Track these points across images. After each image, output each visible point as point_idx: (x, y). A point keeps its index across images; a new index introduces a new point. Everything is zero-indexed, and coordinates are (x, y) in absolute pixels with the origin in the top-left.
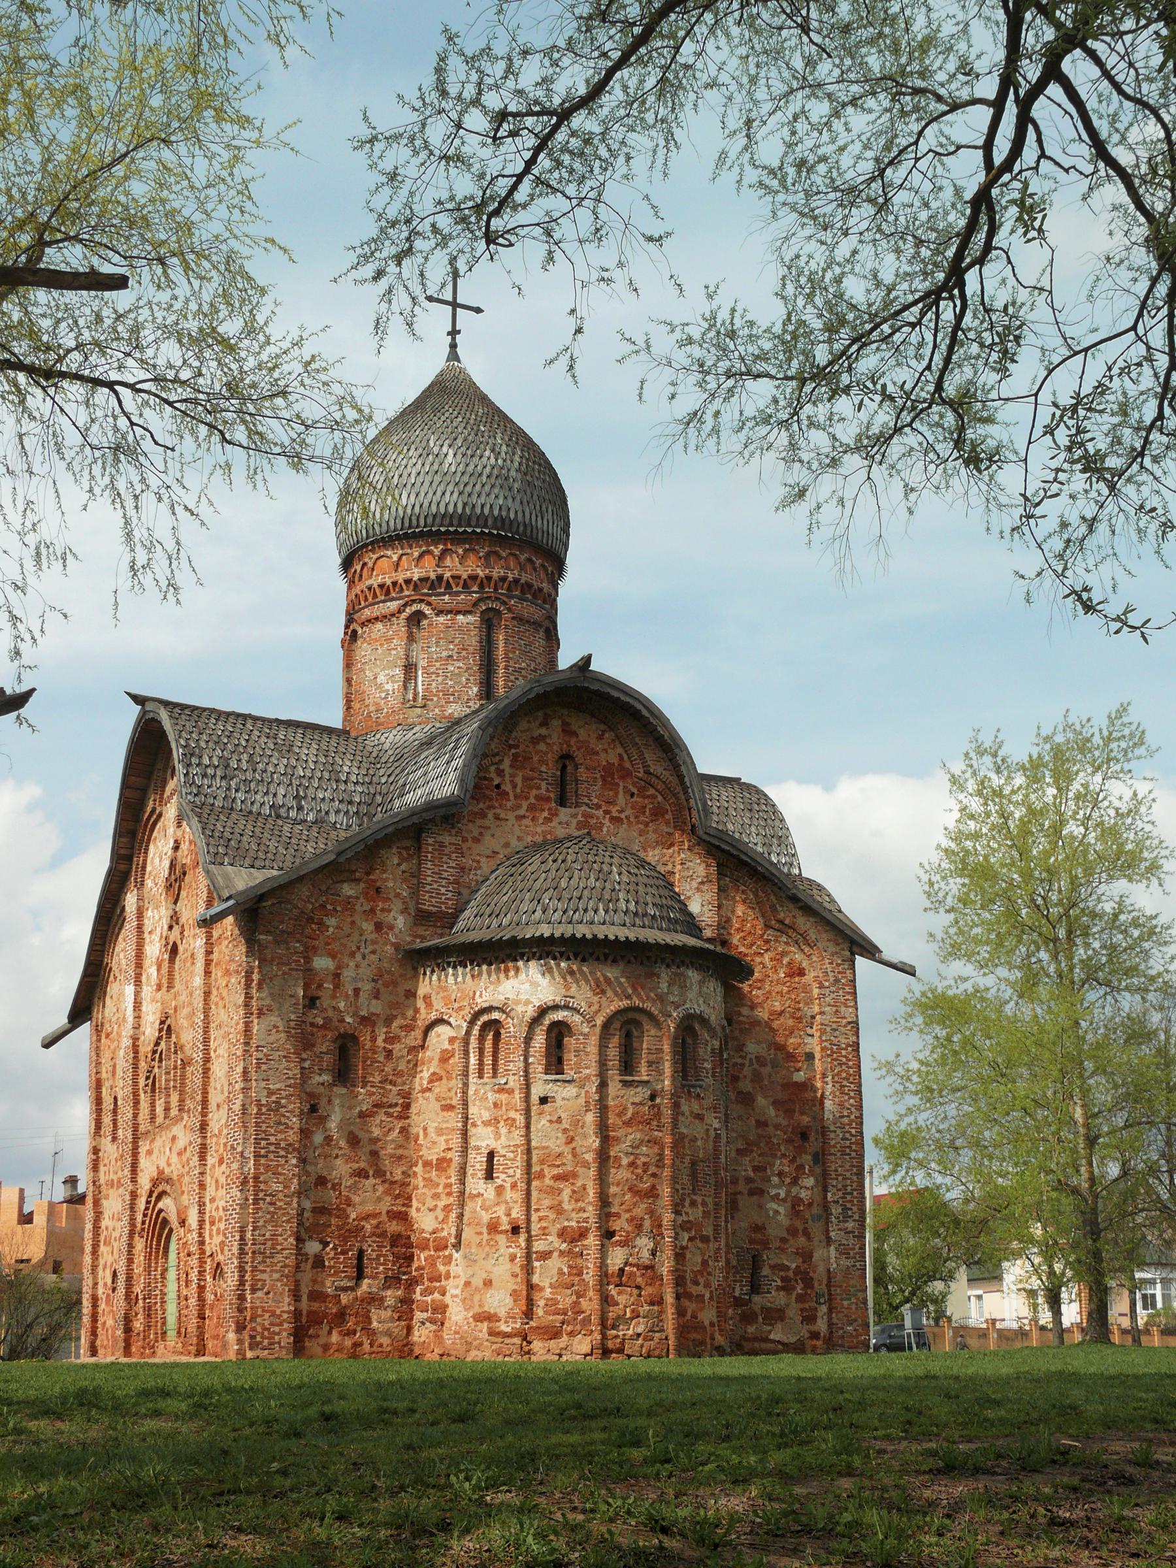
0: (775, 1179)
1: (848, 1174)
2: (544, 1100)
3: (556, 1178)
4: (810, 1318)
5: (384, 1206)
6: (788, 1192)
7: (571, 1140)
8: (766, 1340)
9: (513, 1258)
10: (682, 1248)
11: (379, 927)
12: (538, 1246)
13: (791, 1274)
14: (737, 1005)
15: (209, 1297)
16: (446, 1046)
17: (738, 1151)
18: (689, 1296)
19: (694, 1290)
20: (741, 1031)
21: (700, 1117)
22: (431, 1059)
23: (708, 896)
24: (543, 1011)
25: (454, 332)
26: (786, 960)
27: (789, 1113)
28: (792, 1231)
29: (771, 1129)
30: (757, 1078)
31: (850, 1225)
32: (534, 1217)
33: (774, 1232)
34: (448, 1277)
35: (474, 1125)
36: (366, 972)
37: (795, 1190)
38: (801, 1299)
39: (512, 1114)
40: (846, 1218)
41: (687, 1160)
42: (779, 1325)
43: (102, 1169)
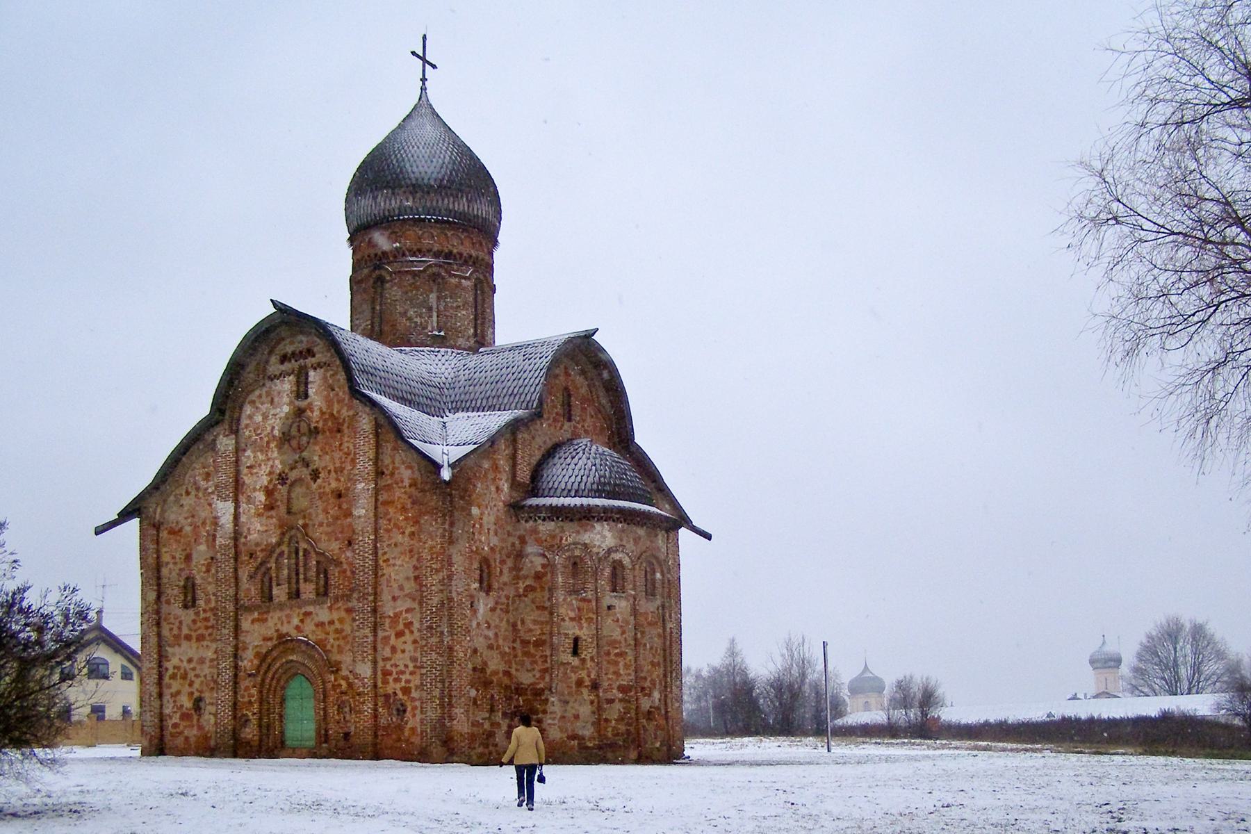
2: (609, 608)
3: (617, 655)
5: (502, 667)
7: (623, 633)
9: (592, 702)
11: (498, 489)
12: (609, 696)
15: (383, 722)
16: (539, 568)
22: (526, 577)
24: (610, 551)
25: (424, 80)
32: (605, 677)
34: (545, 712)
35: (563, 620)
36: (492, 519)
39: (591, 615)
43: (164, 624)
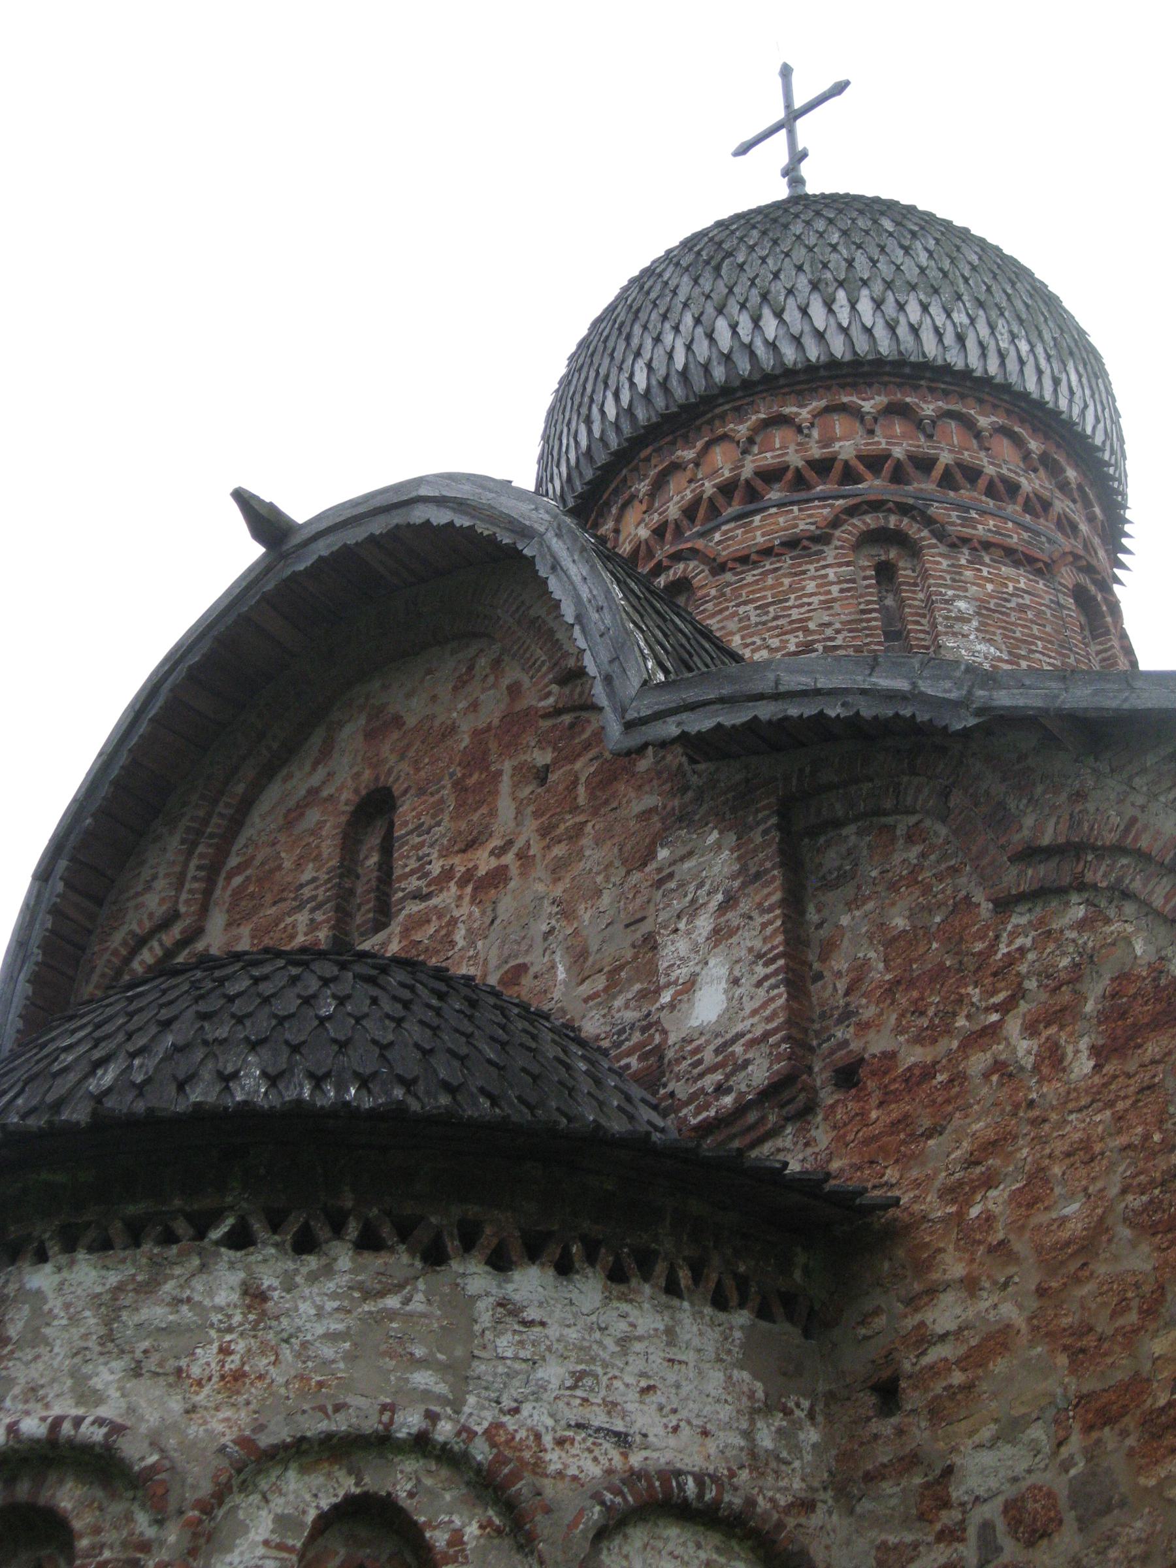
14: (913, 1302)
20: (935, 1413)
23: (749, 939)
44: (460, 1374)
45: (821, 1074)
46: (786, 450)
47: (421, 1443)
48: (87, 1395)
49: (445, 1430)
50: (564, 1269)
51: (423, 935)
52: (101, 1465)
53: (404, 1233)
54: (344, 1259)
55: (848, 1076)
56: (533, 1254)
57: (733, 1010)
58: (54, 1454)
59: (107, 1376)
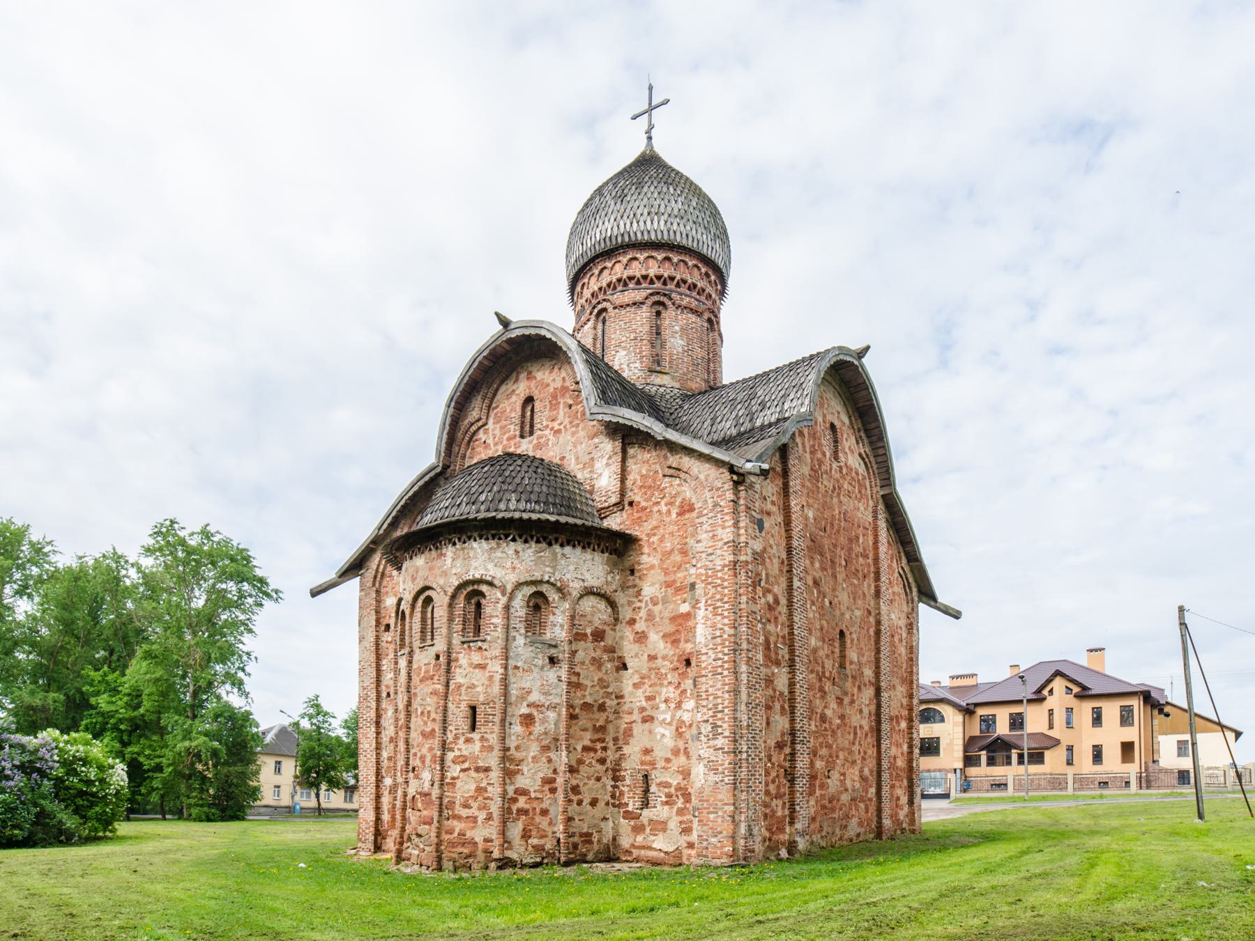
0: (663, 706)
1: (720, 693)
4: (687, 831)
6: (673, 717)
8: (650, 848)
10: (453, 778)
13: (672, 790)
17: (636, 686)
18: (458, 817)
19: (464, 813)
21: (482, 667)
26: (679, 500)
27: (675, 642)
28: (676, 752)
29: (659, 662)
30: (650, 617)
31: (720, 742)
33: (659, 754)
37: (679, 713)
38: (680, 812)
40: (716, 735)
41: (464, 705)
42: (661, 835)
44: (554, 568)
45: (626, 503)
46: (636, 270)
47: (548, 582)
48: (487, 570)
49: (552, 580)
50: (574, 546)
51: (542, 441)
52: (490, 584)
53: (545, 539)
54: (533, 544)
55: (631, 504)
56: (568, 544)
57: (609, 484)
58: (481, 581)
59: (490, 566)
